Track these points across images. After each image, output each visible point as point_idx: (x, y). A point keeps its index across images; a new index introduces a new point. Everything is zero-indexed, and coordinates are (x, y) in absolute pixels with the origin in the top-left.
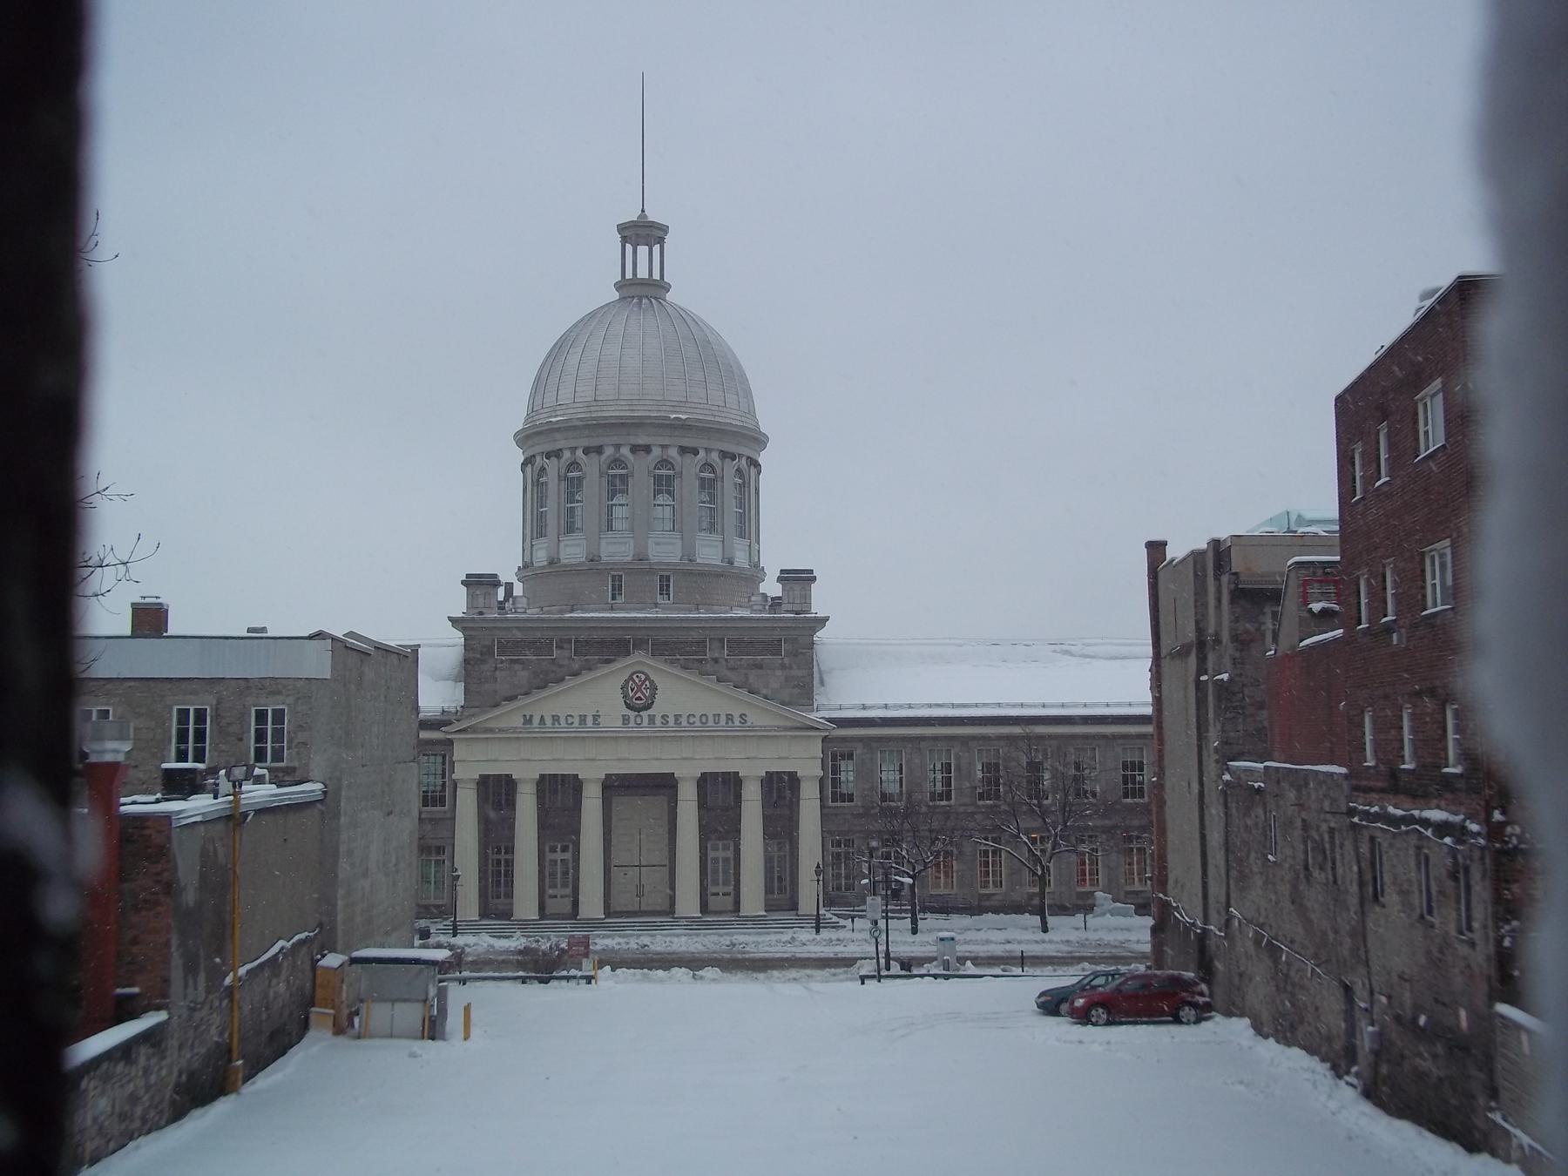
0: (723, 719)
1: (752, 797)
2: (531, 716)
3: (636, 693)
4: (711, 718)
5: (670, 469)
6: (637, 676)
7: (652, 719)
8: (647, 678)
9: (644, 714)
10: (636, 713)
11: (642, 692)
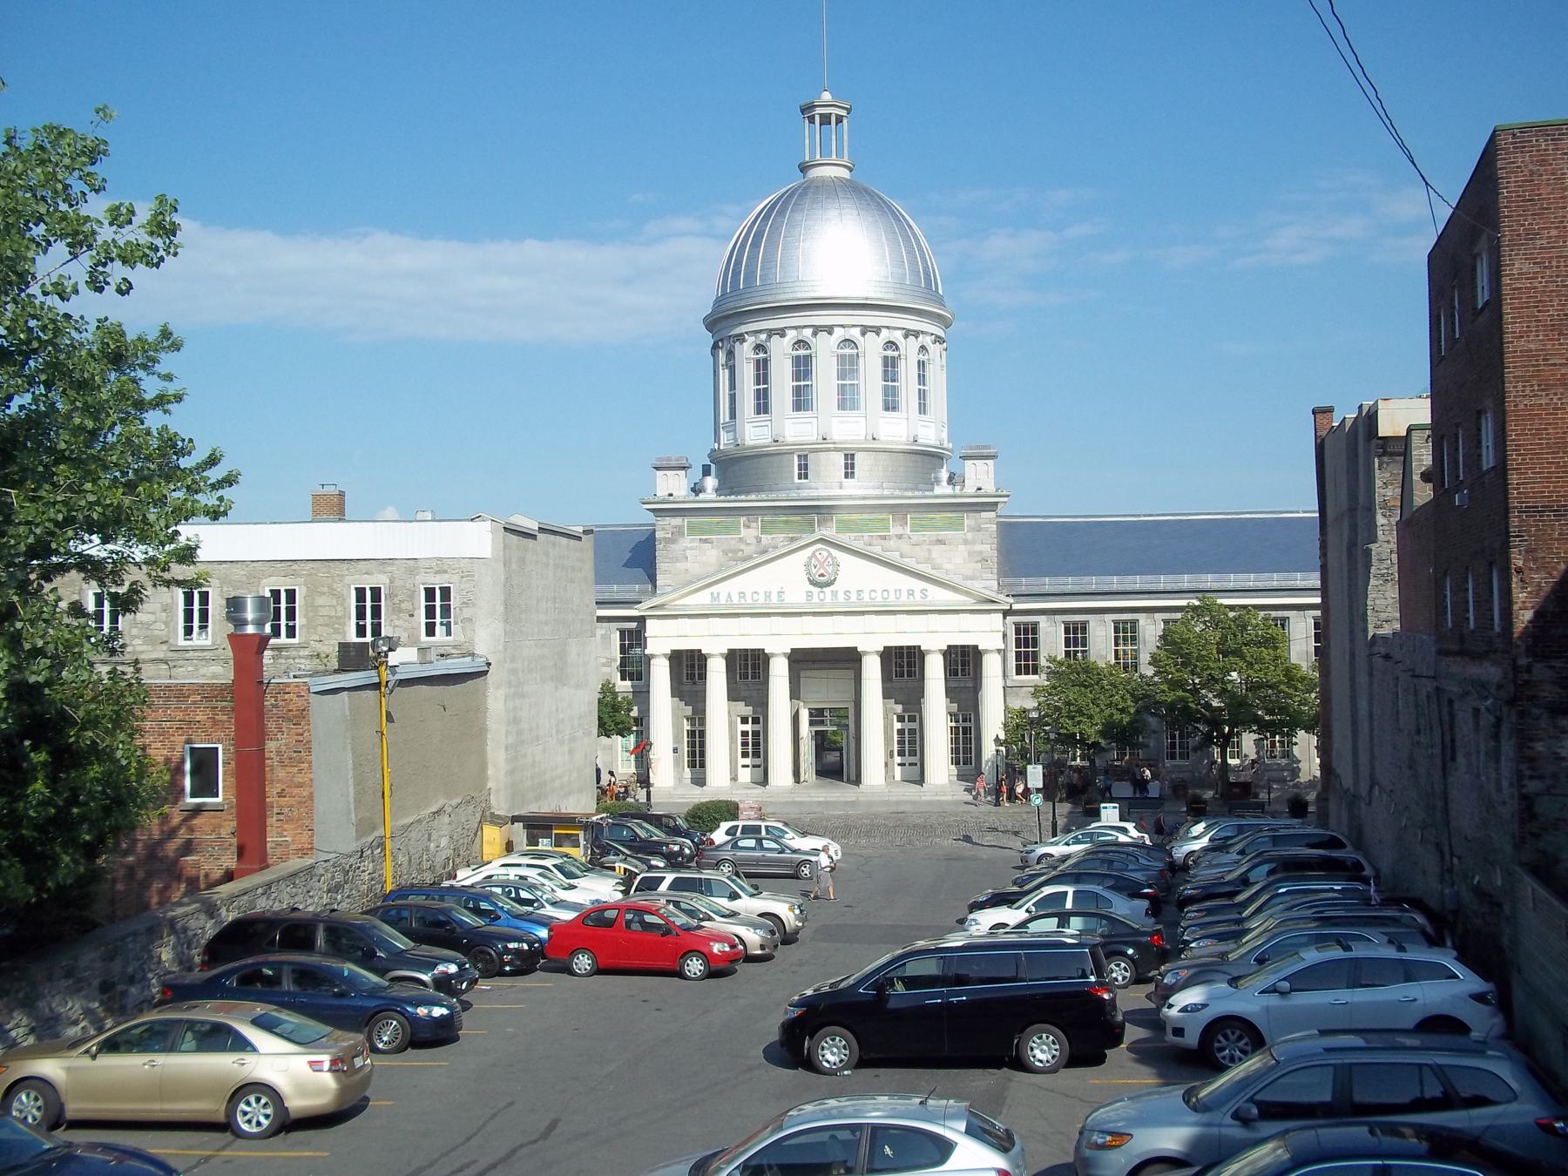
0: (904, 594)
1: (935, 670)
2: (718, 594)
4: (892, 593)
5: (852, 348)
7: (835, 594)
8: (830, 554)
11: (824, 569)
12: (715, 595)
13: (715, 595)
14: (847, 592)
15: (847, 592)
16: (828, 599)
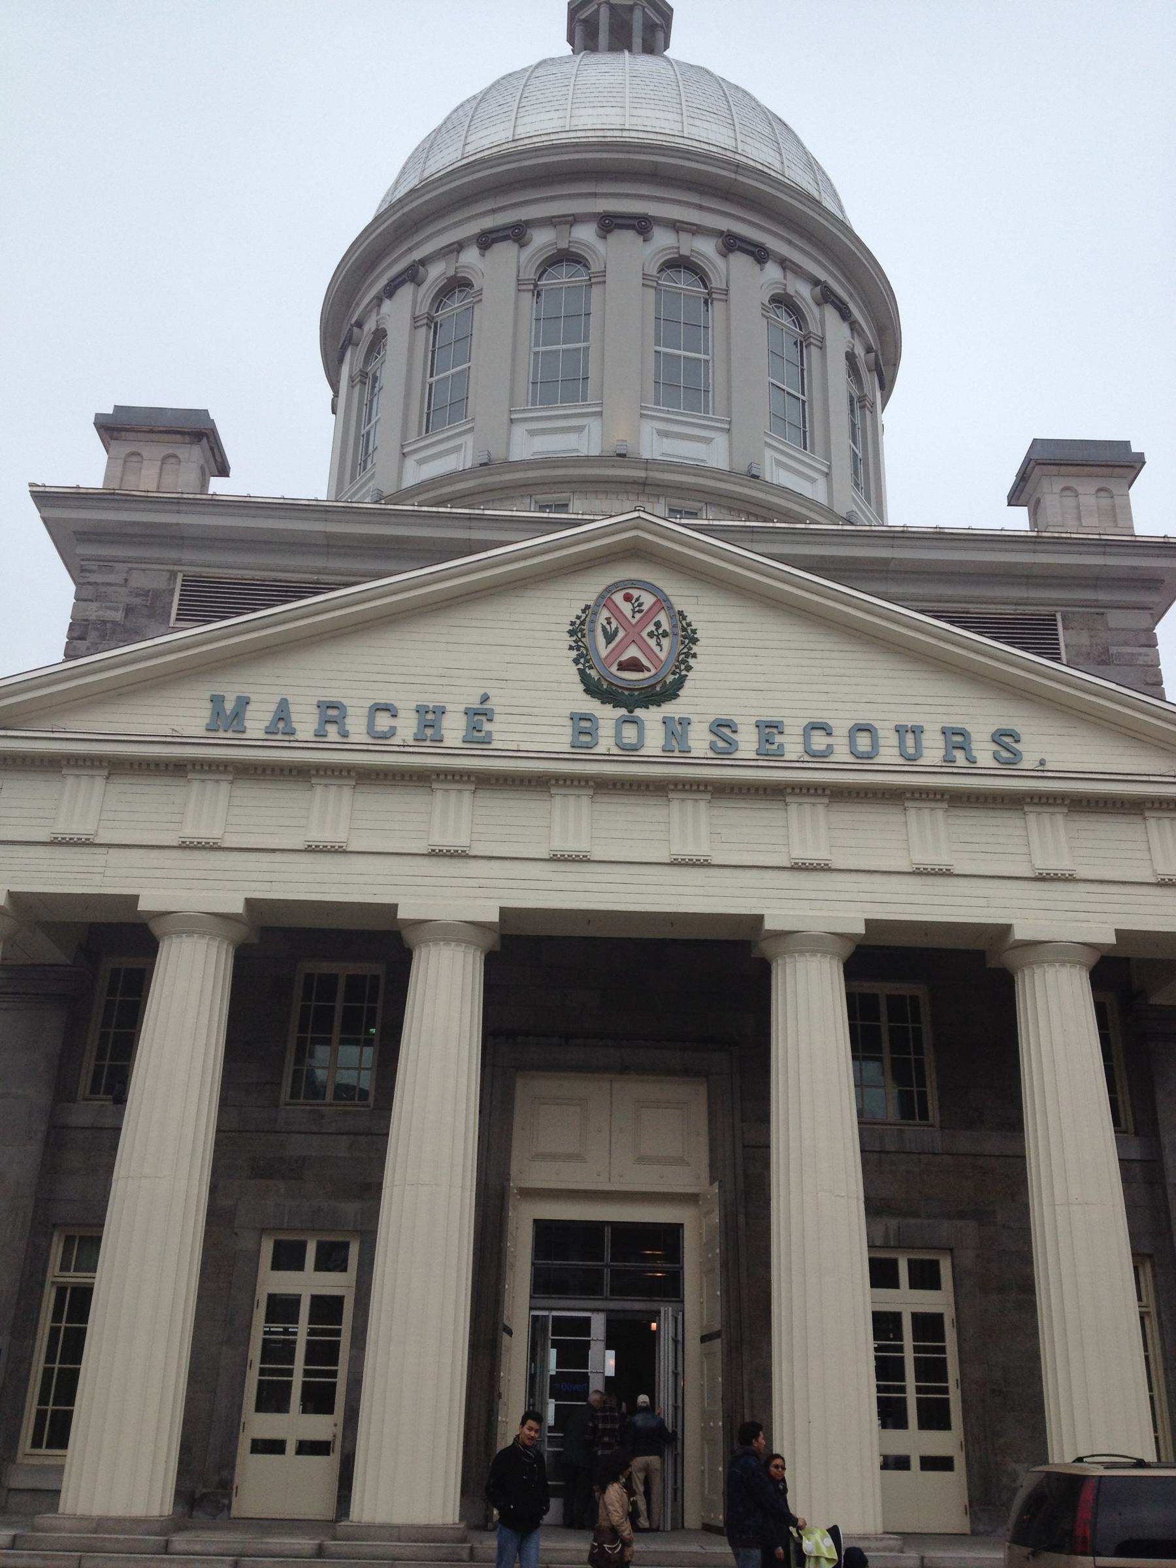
2: (244, 702)
3: (623, 646)
6: (628, 598)
7: (676, 729)
8: (663, 602)
9: (651, 716)
10: (622, 712)
12: (229, 706)
13: (229, 706)
14: (722, 727)
15: (722, 727)
16: (654, 741)
